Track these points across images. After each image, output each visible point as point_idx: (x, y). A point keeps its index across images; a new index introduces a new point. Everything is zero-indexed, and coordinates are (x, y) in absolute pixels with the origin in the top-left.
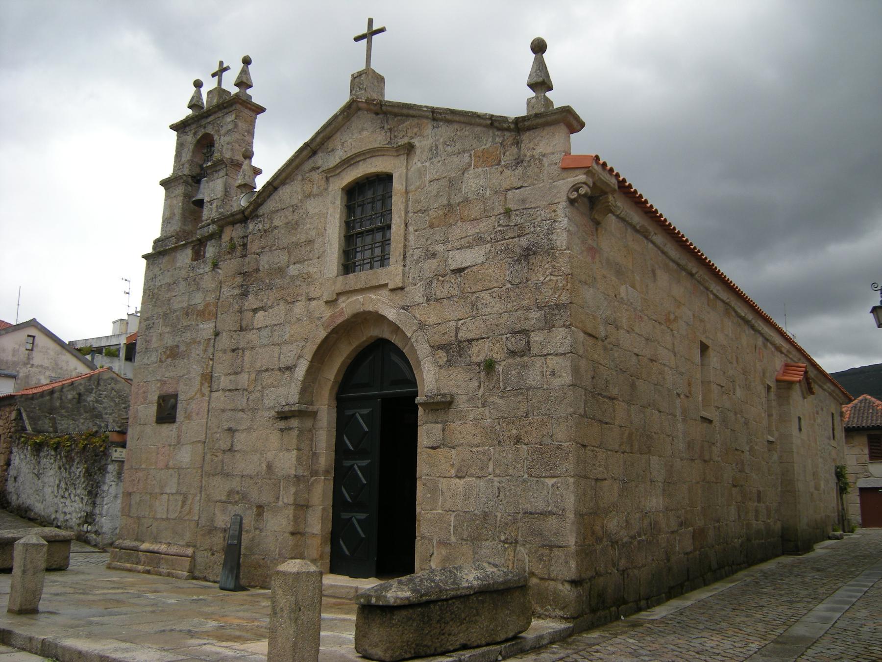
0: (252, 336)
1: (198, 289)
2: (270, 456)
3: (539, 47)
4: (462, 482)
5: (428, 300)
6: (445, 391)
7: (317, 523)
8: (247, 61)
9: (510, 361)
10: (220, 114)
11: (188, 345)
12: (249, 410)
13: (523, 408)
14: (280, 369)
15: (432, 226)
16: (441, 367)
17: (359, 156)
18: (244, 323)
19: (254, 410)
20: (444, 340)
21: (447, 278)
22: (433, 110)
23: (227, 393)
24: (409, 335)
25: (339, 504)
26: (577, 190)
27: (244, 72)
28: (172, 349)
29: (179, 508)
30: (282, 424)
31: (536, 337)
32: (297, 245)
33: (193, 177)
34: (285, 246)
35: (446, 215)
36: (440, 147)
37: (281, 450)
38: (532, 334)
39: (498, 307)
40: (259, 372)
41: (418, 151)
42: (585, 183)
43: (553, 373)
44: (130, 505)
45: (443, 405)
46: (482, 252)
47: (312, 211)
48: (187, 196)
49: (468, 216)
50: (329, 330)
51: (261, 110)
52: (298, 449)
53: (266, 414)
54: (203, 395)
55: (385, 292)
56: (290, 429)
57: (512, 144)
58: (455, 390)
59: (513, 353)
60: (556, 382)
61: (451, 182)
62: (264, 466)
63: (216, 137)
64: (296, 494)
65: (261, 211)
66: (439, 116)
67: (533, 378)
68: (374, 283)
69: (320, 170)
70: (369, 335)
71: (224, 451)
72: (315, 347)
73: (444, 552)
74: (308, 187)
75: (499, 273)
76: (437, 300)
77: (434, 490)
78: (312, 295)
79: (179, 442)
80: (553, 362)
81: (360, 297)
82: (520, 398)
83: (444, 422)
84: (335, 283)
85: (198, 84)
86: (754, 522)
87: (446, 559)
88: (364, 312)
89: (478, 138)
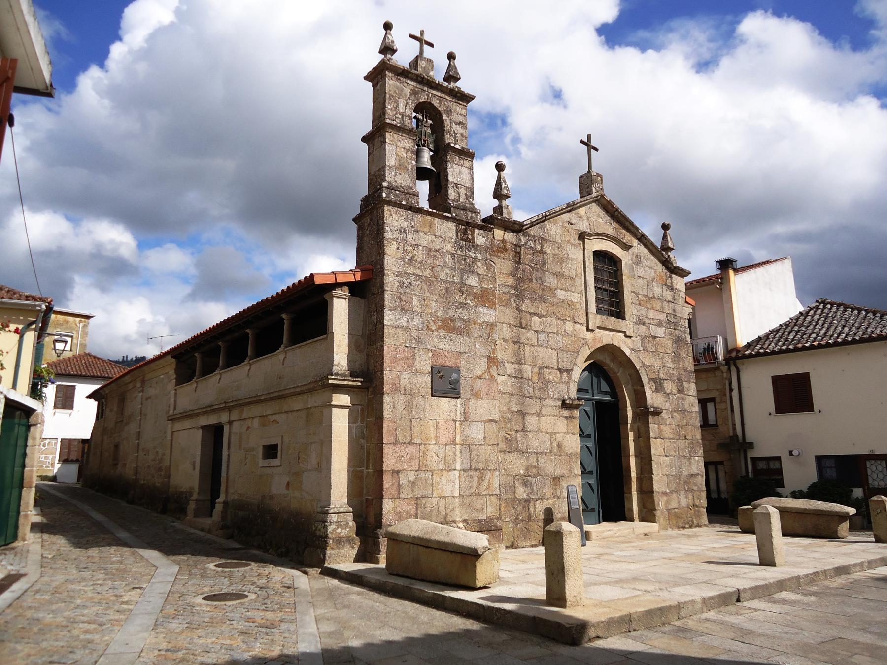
0: (531, 334)
2: (559, 438)
8: (451, 56)
14: (559, 369)
18: (524, 322)
22: (643, 236)
23: (513, 379)
28: (444, 321)
29: (475, 484)
30: (566, 413)
40: (541, 368)
44: (399, 486)
55: (622, 335)
62: (555, 444)
78: (576, 319)
79: (466, 419)
83: (658, 424)
87: (668, 502)
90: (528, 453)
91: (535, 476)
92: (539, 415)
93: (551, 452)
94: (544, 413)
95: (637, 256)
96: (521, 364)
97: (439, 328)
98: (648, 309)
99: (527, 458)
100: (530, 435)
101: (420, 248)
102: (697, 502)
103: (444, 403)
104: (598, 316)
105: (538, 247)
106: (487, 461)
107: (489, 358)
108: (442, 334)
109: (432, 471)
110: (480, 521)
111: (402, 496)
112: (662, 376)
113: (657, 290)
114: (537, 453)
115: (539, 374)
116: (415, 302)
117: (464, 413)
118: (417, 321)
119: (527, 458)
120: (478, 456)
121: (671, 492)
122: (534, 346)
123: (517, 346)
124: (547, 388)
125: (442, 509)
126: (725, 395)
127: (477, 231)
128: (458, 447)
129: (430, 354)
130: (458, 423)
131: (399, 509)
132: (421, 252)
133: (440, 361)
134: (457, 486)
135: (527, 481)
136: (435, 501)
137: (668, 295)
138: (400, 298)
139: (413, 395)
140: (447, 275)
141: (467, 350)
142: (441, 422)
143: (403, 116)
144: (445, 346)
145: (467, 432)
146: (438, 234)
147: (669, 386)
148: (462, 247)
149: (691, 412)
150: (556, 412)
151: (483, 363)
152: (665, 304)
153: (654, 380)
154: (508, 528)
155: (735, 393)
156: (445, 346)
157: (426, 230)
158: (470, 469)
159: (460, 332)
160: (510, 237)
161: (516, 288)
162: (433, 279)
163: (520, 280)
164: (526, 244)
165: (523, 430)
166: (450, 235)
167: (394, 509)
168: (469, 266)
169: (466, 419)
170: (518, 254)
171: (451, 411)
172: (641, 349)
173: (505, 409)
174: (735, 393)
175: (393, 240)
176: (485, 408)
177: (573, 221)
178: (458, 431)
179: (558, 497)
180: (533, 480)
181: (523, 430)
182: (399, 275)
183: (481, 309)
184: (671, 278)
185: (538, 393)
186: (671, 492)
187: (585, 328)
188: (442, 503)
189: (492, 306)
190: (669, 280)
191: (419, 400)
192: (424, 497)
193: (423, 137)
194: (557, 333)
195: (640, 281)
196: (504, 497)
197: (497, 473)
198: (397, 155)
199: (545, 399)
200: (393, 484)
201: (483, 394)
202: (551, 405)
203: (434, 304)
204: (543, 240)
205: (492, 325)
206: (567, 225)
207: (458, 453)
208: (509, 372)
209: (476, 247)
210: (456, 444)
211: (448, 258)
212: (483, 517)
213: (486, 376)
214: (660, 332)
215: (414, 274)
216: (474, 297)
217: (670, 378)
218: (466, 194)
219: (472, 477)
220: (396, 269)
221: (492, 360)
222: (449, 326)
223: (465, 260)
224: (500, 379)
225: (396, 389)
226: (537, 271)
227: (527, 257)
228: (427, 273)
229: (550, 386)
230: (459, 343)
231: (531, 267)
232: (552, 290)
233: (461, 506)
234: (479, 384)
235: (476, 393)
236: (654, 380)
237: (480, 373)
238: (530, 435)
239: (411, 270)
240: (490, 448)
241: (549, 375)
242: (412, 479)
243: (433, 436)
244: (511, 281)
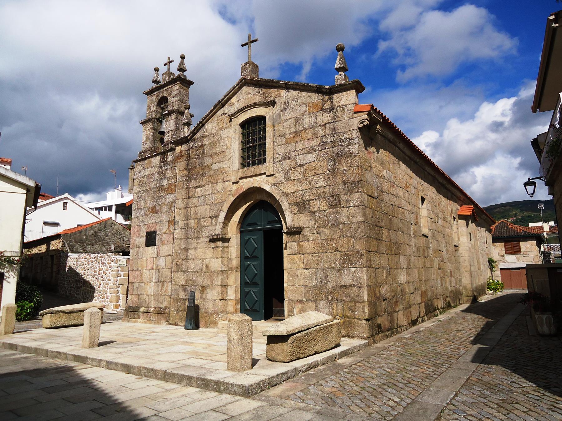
0: (195, 200)
1: (164, 178)
2: (207, 261)
4: (308, 271)
5: (287, 180)
6: (297, 225)
7: (233, 294)
8: (183, 57)
9: (331, 210)
11: (160, 206)
13: (338, 233)
14: (210, 217)
15: (287, 143)
16: (295, 214)
17: (247, 108)
19: (198, 238)
20: (296, 201)
21: (296, 169)
23: (183, 230)
24: (277, 198)
25: (244, 284)
26: (362, 123)
27: (182, 63)
28: (152, 209)
29: (160, 289)
30: (213, 245)
31: (343, 198)
32: (216, 154)
33: (157, 119)
34: (210, 154)
35: (294, 137)
36: (290, 102)
38: (341, 197)
39: (323, 184)
40: (200, 219)
41: (278, 104)
42: (367, 119)
43: (353, 216)
45: (295, 232)
46: (314, 156)
47: (223, 136)
48: (155, 129)
49: (306, 137)
50: (236, 197)
51: (192, 83)
52: (222, 257)
53: (204, 240)
54: (170, 231)
55: (264, 176)
56: (217, 247)
57: (328, 100)
58: (303, 226)
59: (331, 206)
60: (355, 220)
61: (297, 120)
62: (204, 266)
63: (169, 98)
64: (222, 279)
65: (196, 137)
67: (343, 218)
68: (258, 173)
69: (227, 115)
71: (183, 260)
72: (228, 206)
73: (300, 306)
74: (221, 124)
75: (323, 166)
77: (294, 276)
78: (225, 179)
79: (158, 256)
80: (352, 210)
81: (251, 179)
82: (336, 229)
83: (298, 242)
84: (237, 173)
85: (157, 70)
86: (449, 287)
89: (310, 97)
91: (191, 285)
93: (201, 271)
100: (190, 261)
105: (200, 144)
123: (186, 210)
125: (147, 301)
136: (145, 296)
139: (139, 248)
142: (148, 258)
145: (158, 263)
150: (206, 245)
154: (173, 313)
158: (158, 282)
163: (190, 170)
165: (186, 259)
169: (158, 256)
179: (204, 299)
181: (186, 259)
186: (308, 301)
189: (173, 191)
191: (141, 249)
196: (173, 296)
201: (166, 242)
203: (149, 202)
208: (180, 226)
212: (163, 306)
217: (320, 197)
221: (173, 223)
232: (209, 167)
233: (154, 300)
234: (164, 236)
238: (190, 261)
244: (185, 172)
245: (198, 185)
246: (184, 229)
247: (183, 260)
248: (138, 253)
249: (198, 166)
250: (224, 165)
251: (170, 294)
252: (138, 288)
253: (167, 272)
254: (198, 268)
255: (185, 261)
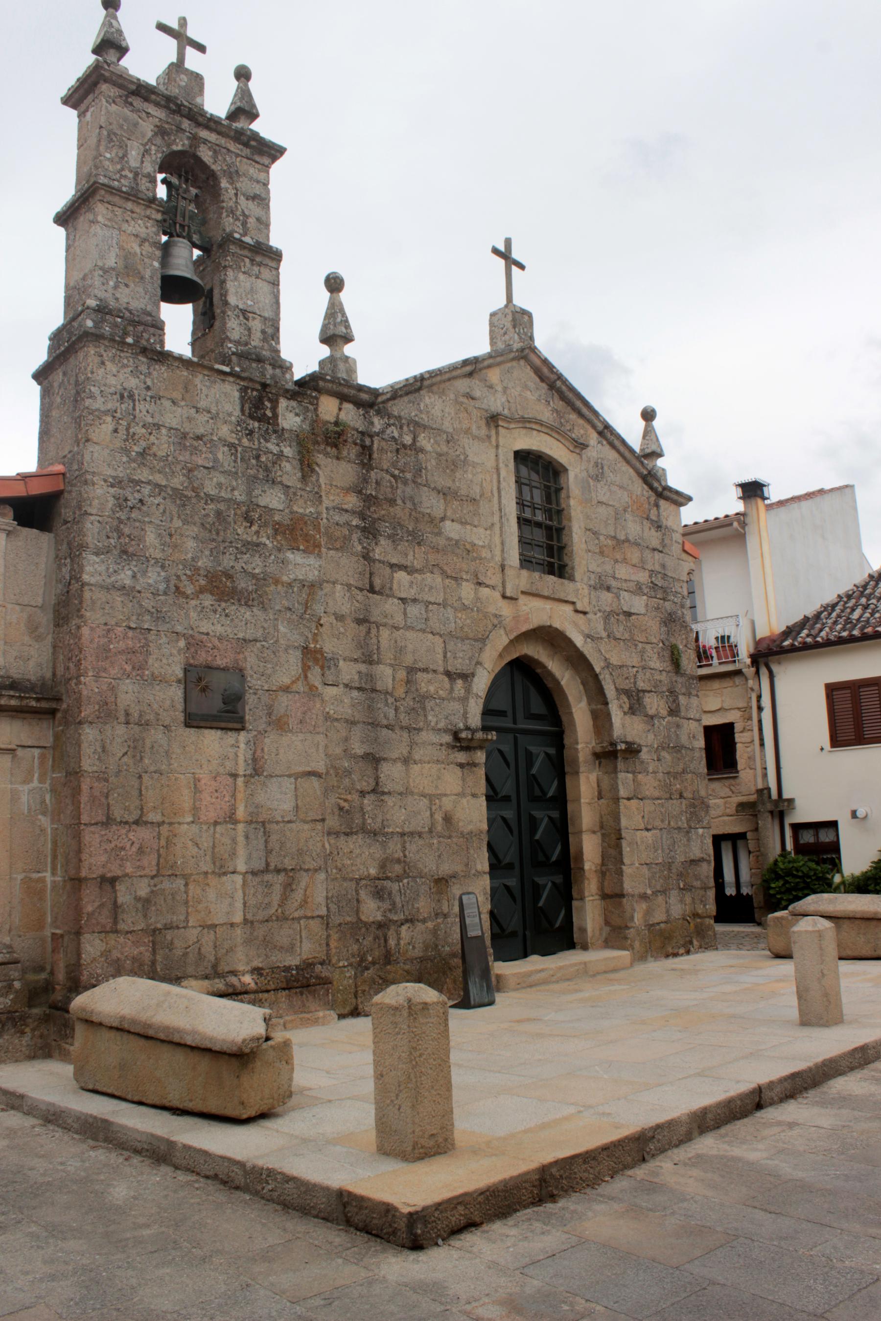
0: (391, 606)
2: (447, 803)
3: (334, 284)
5: (609, 636)
10: (233, 146)
11: (261, 580)
12: (402, 728)
14: (448, 674)
17: (536, 423)
18: (377, 582)
22: (607, 427)
23: (355, 693)
29: (276, 898)
30: (462, 757)
37: (462, 795)
40: (412, 670)
53: (435, 738)
55: (568, 608)
62: (439, 817)
66: (608, 435)
68: (562, 596)
70: (523, 653)
71: (363, 794)
73: (644, 906)
76: (616, 639)
78: (482, 579)
83: (634, 773)
87: (648, 913)
88: (550, 626)
90: (385, 835)
91: (399, 879)
92: (406, 761)
93: (430, 831)
94: (417, 757)
95: (596, 464)
96: (371, 663)
97: (202, 591)
98: (616, 561)
99: (384, 845)
101: (164, 431)
102: (700, 910)
103: (212, 741)
104: (525, 573)
106: (300, 852)
107: (306, 650)
108: (207, 603)
109: (186, 877)
110: (288, 969)
111: (122, 926)
112: (641, 685)
113: (633, 528)
114: (403, 834)
115: (408, 682)
116: (151, 538)
117: (255, 760)
118: (154, 577)
119: (384, 845)
120: (282, 844)
121: (655, 893)
122: (397, 628)
123: (363, 629)
124: (424, 709)
125: (208, 950)
126: (750, 718)
127: (283, 403)
128: (241, 827)
129: (182, 644)
130: (240, 781)
131: (115, 954)
132: (164, 439)
133: (203, 657)
134: (239, 905)
135: (383, 889)
136: (192, 934)
137: (653, 538)
138: (118, 530)
140: (220, 485)
141: (259, 634)
142: (205, 779)
143: (136, 174)
144: (213, 626)
145: (261, 798)
146: (202, 404)
147: (654, 704)
148: (251, 433)
149: (692, 749)
150: (443, 754)
151: (292, 663)
152: (648, 554)
153: (627, 693)
155: (767, 715)
156: (213, 626)
157: (176, 395)
158: (266, 870)
159: (245, 599)
160: (350, 415)
161: (362, 516)
162: (190, 493)
164: (383, 432)
165: (374, 791)
166: (228, 407)
167: (106, 954)
168: (267, 470)
170: (366, 451)
171: (226, 757)
172: (604, 634)
173: (338, 751)
174: (767, 715)
175: (106, 412)
176: (297, 749)
177: (477, 393)
178: (240, 796)
180: (395, 887)
181: (374, 791)
182: (117, 483)
183: (290, 555)
184: (657, 506)
185: (405, 719)
187: (497, 595)
188: (208, 938)
189: (313, 548)
190: (654, 511)
191: (156, 735)
192: (168, 927)
193: (179, 219)
194: (444, 604)
195: (602, 510)
196: (336, 920)
197: (322, 876)
198: (121, 248)
199: (419, 730)
200: (102, 905)
201: (293, 723)
202: (432, 742)
203: (191, 544)
204: (417, 426)
205: (312, 587)
206: (465, 400)
207: (241, 839)
208: (345, 678)
209: (280, 433)
210: (236, 822)
211: (223, 454)
212: (293, 961)
213: (300, 686)
214: (638, 604)
215: (149, 483)
216: (276, 531)
218: (263, 332)
219: (269, 885)
220: (110, 472)
221: (311, 655)
222: (222, 588)
223: (257, 457)
224: (332, 691)
225: (107, 713)
226: (405, 483)
227: (385, 458)
228: (178, 481)
229: (429, 704)
230: (245, 621)
231: (394, 476)
232: (435, 522)
233: (248, 942)
234: (284, 701)
235: (279, 720)
236: (627, 693)
237: (287, 681)
239: (143, 474)
240: (306, 827)
241: (426, 684)
242: (143, 892)
243: (187, 806)
244: (352, 501)
245: (403, 562)
246: (359, 689)
247: (363, 794)
248: (136, 748)
249: (399, 502)
250: (478, 536)
251: (323, 911)
252: (146, 903)
253: (310, 839)
254: (421, 822)
255: (372, 797)
